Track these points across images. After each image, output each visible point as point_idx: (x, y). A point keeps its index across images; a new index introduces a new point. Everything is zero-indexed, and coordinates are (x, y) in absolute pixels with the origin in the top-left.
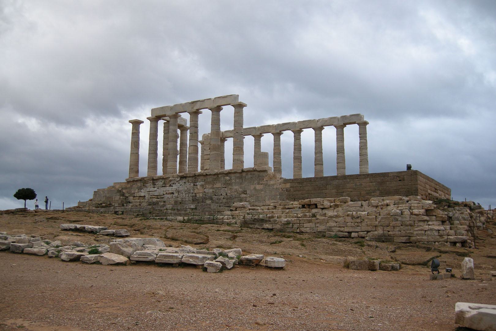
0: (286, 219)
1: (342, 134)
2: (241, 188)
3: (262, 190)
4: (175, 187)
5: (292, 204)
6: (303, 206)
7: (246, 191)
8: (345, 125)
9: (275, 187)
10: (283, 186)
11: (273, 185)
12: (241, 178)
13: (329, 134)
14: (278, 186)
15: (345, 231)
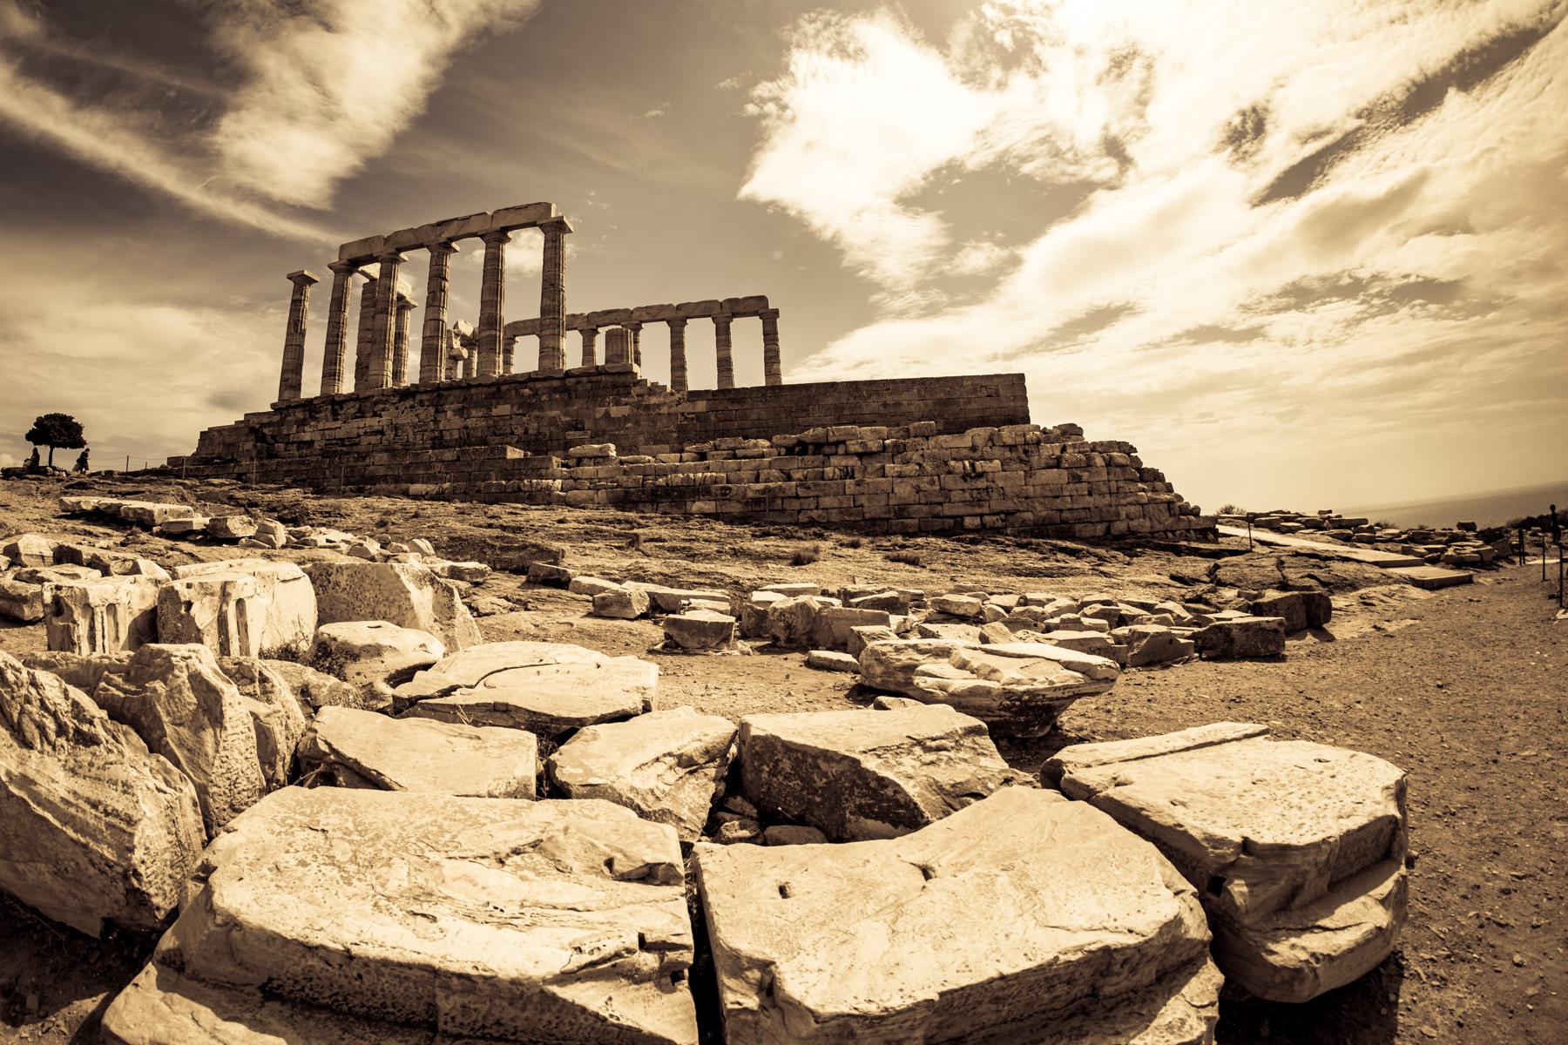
0: (760, 486)
1: (728, 333)
2: (566, 415)
3: (626, 419)
4: (385, 418)
5: (755, 446)
6: (790, 451)
7: (582, 422)
8: (735, 315)
9: (664, 410)
10: (686, 407)
11: (658, 406)
12: (564, 389)
13: (700, 334)
14: (673, 410)
15: (947, 513)
